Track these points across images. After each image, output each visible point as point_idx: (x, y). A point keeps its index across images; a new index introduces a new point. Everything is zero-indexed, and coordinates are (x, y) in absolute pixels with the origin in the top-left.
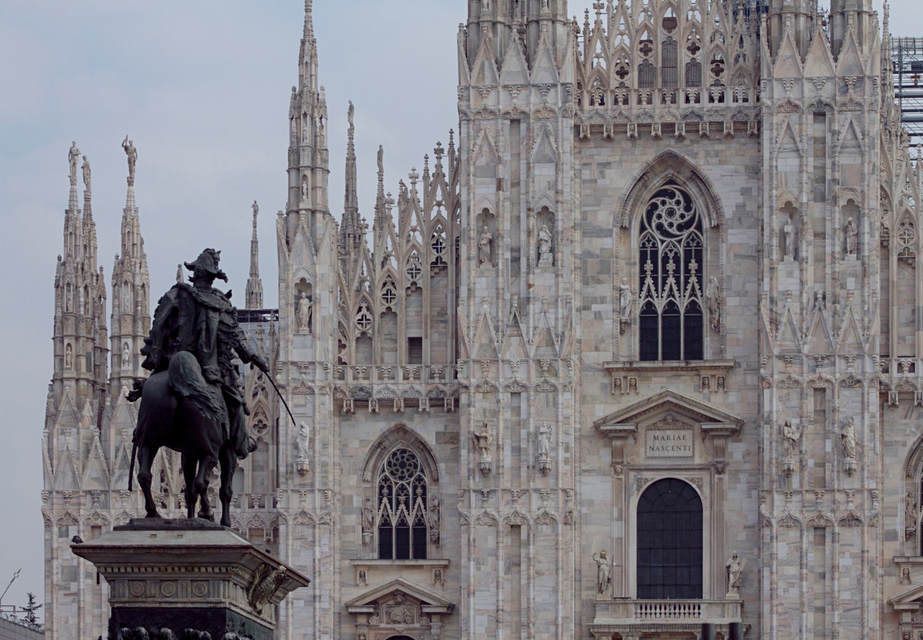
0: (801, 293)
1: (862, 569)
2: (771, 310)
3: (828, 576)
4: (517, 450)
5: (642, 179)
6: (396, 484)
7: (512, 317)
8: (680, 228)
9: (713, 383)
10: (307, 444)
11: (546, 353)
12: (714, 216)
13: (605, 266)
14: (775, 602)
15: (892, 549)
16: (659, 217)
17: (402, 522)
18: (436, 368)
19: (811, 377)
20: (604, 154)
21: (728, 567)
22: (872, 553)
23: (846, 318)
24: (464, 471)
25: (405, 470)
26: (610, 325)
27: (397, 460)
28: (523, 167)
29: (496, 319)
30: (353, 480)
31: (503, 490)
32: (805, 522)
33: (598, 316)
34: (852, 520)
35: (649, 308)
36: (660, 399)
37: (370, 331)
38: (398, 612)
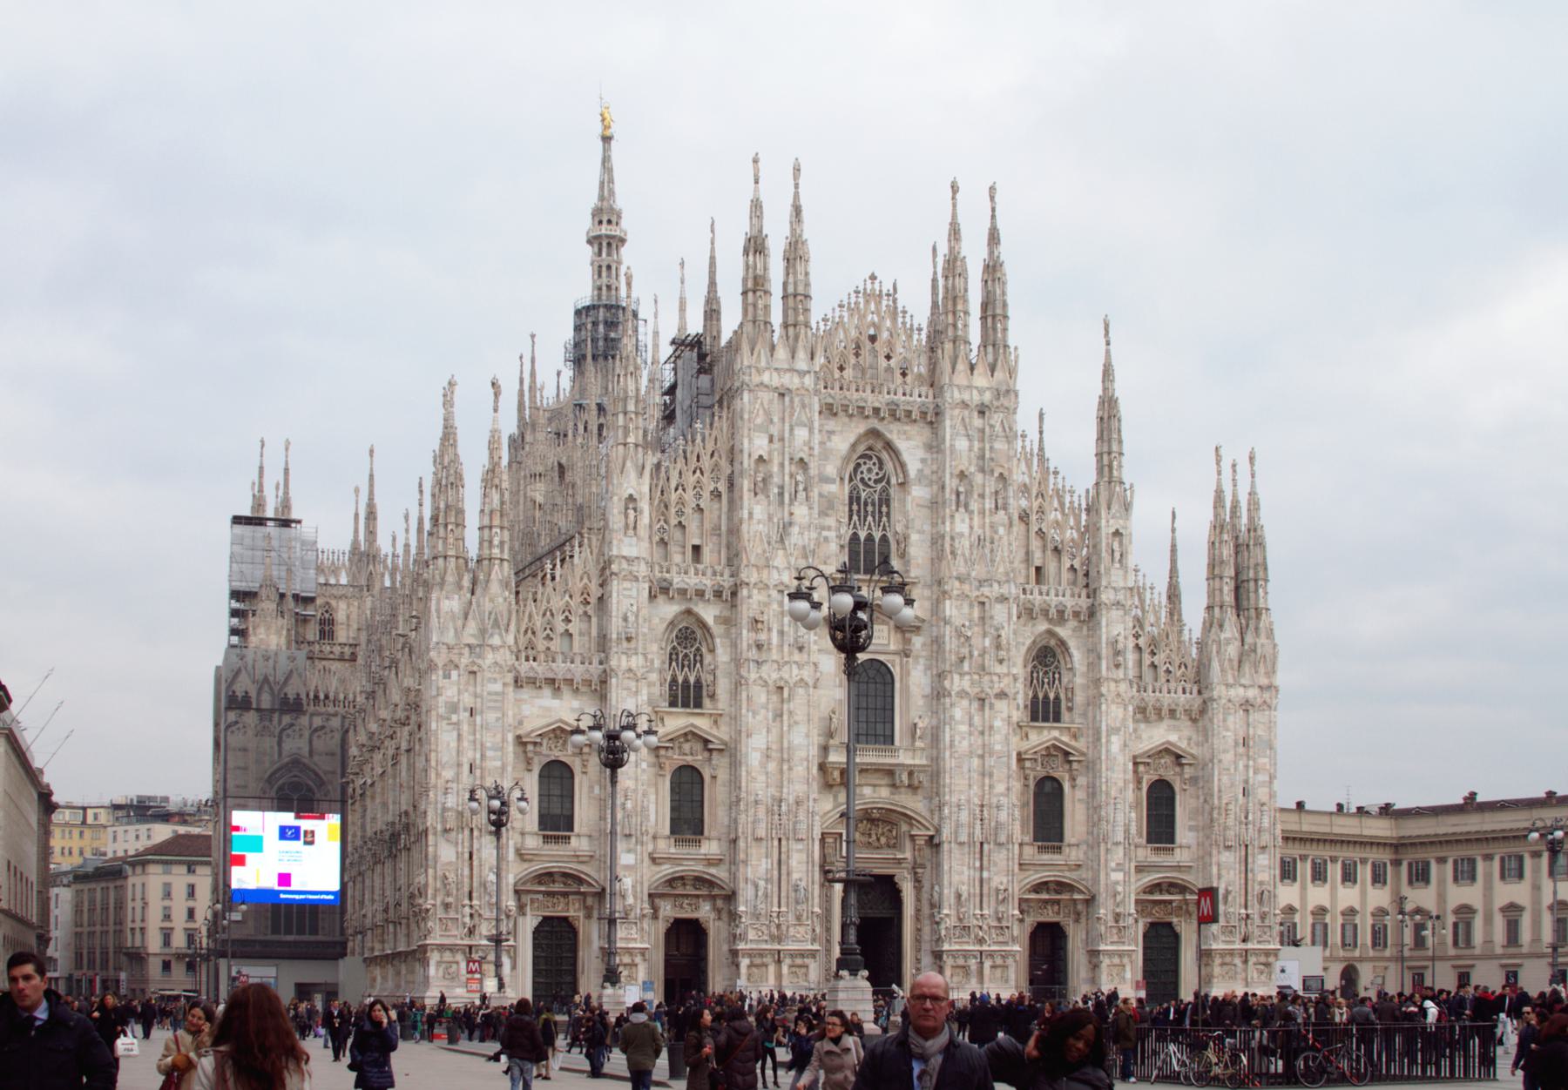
4: (781, 633)
5: (854, 446)
8: (876, 481)
17: (686, 681)
24: (745, 645)
26: (833, 547)
28: (787, 428)
29: (769, 537)
30: (655, 647)
33: (826, 539)
34: (1002, 695)
35: (855, 537)
38: (687, 747)
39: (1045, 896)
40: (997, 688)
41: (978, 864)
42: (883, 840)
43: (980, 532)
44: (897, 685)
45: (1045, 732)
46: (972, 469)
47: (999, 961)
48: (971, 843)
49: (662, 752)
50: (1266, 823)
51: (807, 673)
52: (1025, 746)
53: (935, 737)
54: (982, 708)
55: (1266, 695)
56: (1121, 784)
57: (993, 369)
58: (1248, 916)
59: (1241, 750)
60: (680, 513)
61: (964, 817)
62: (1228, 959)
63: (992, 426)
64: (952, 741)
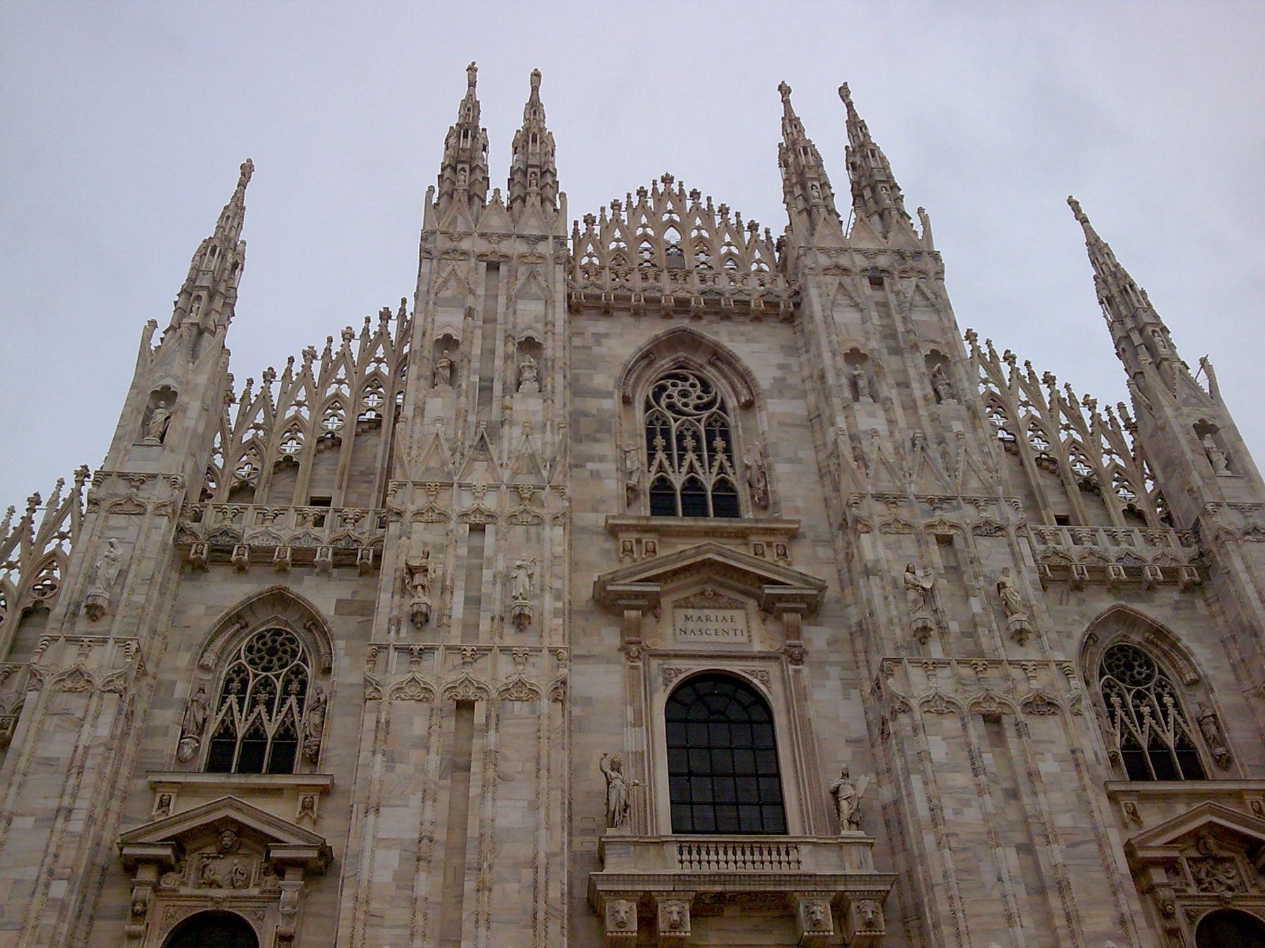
0: (892, 433)
1: (1081, 779)
2: (854, 448)
3: (1024, 789)
5: (648, 356)
6: (256, 676)
7: (478, 438)
9: (770, 556)
10: (113, 572)
11: (527, 480)
12: (745, 391)
13: (603, 425)
14: (942, 829)
16: (670, 397)
17: (256, 733)
18: (350, 512)
19: (929, 520)
20: (602, 326)
21: (835, 792)
23: (962, 457)
24: (381, 620)
25: (275, 659)
26: (612, 486)
27: (265, 644)
28: (502, 300)
30: (184, 659)
31: (448, 648)
32: (964, 701)
33: (596, 475)
34: (1043, 705)
36: (697, 555)
37: (255, 481)
38: (222, 868)
40: (1025, 690)
44: (780, 720)
49: (147, 874)
51: (539, 673)
52: (1133, 833)
53: (895, 821)
54: (998, 739)
63: (897, 293)
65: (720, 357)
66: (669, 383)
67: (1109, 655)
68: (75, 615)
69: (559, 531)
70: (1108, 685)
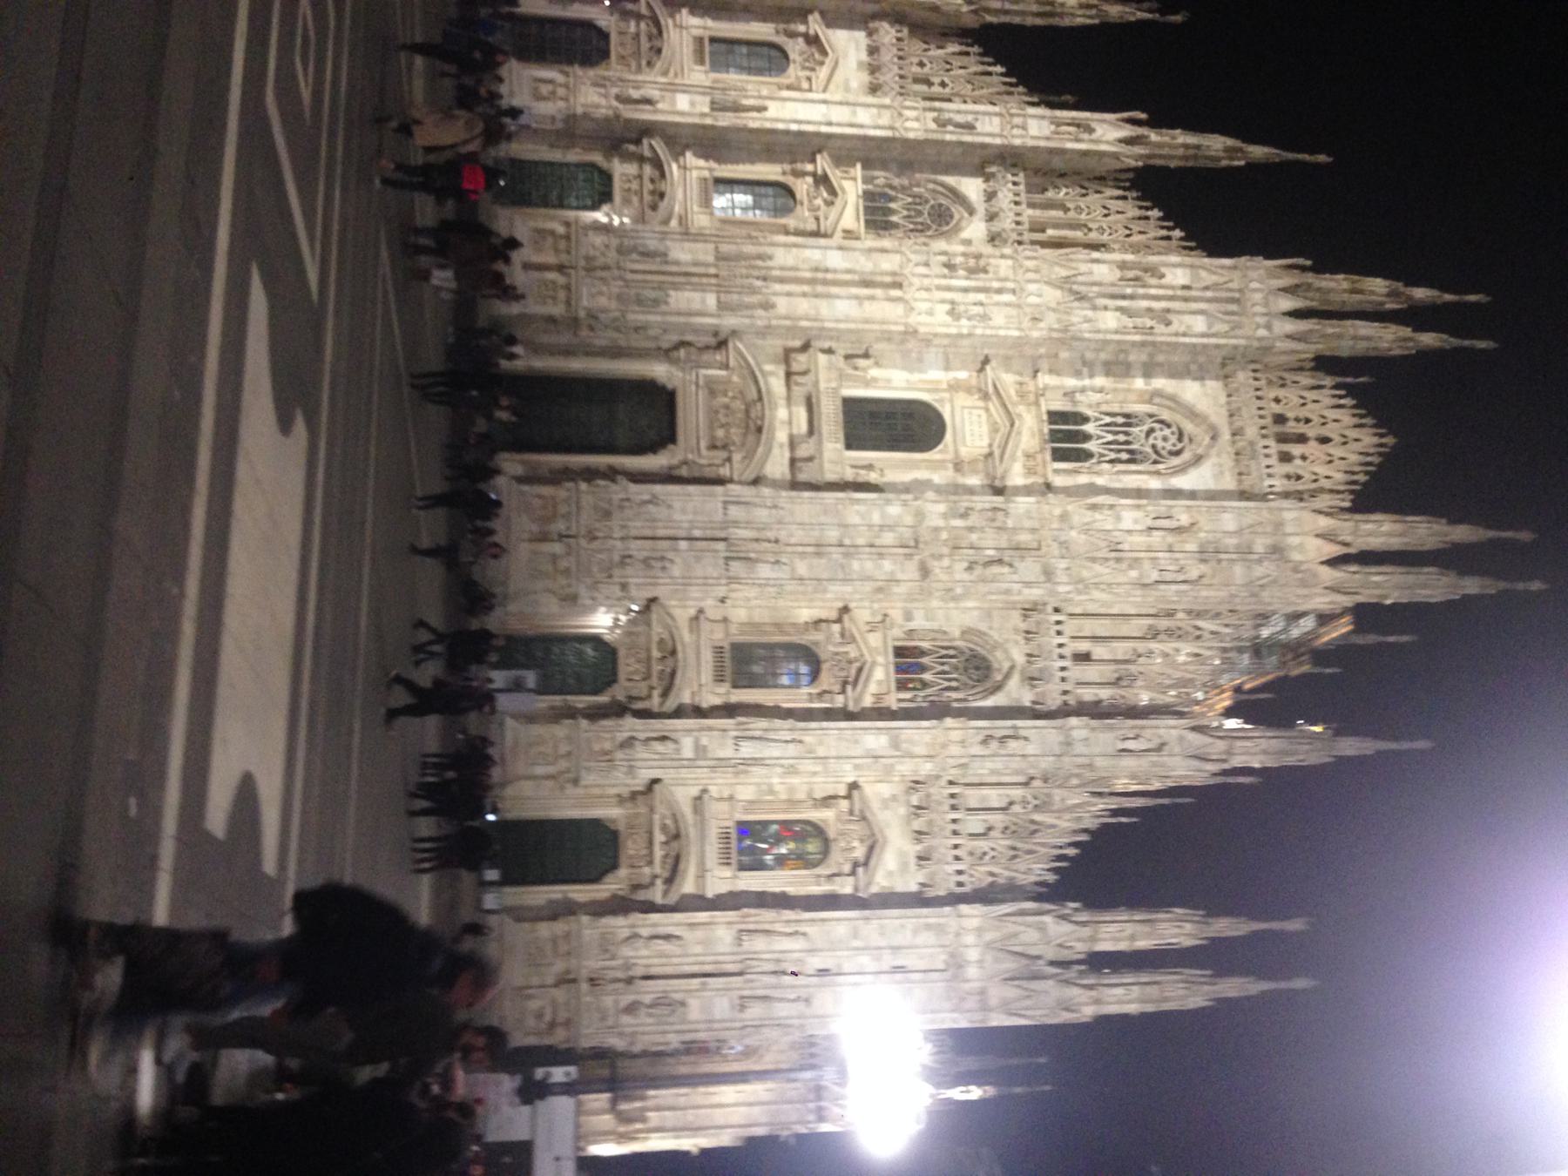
3: (873, 550)
5: (1193, 414)
15: (896, 614)
22: (896, 589)
26: (1071, 382)
34: (925, 572)
39: (656, 654)
41: (697, 533)
42: (720, 433)
43: (1126, 547)
45: (880, 659)
46: (1202, 535)
47: (563, 564)
48: (726, 524)
50: (782, 1010)
55: (971, 1003)
56: (821, 752)
57: (1333, 562)
58: (629, 981)
59: (889, 961)
60: (1079, 209)
61: (762, 514)
62: (563, 948)
63: (1260, 561)
64: (858, 501)
65: (1198, 460)
66: (1174, 429)
67: (984, 659)
68: (934, 110)
69: (1016, 333)
70: (962, 653)
